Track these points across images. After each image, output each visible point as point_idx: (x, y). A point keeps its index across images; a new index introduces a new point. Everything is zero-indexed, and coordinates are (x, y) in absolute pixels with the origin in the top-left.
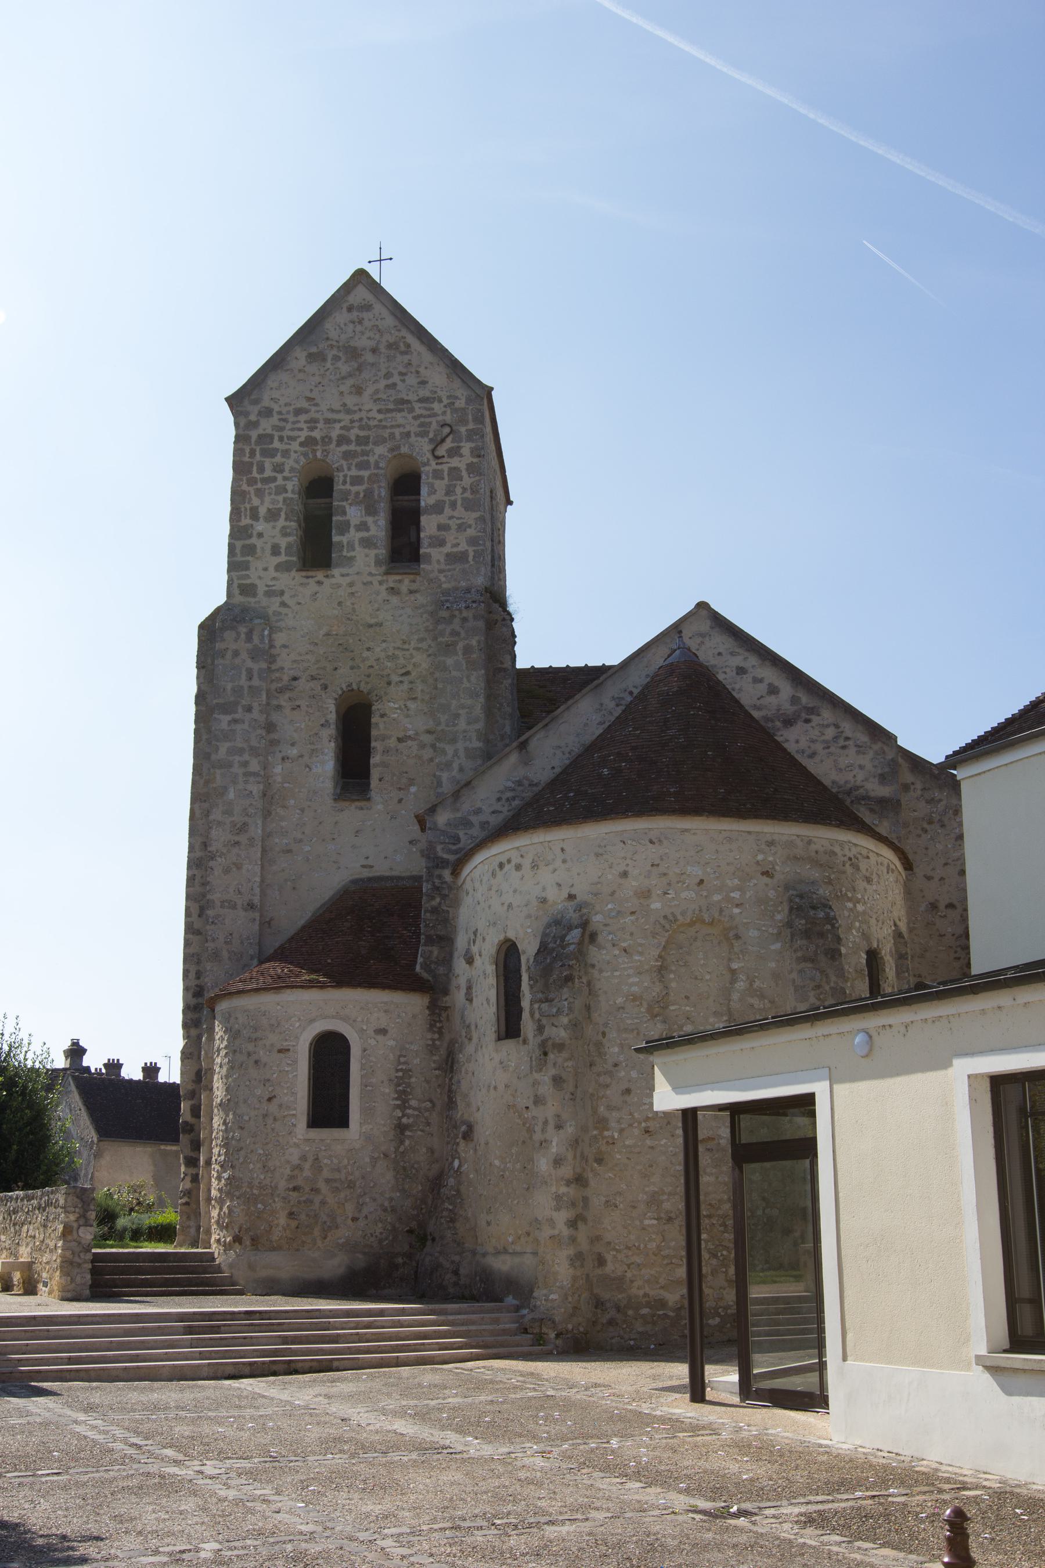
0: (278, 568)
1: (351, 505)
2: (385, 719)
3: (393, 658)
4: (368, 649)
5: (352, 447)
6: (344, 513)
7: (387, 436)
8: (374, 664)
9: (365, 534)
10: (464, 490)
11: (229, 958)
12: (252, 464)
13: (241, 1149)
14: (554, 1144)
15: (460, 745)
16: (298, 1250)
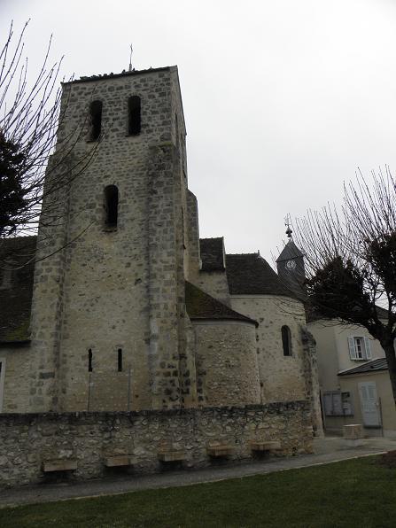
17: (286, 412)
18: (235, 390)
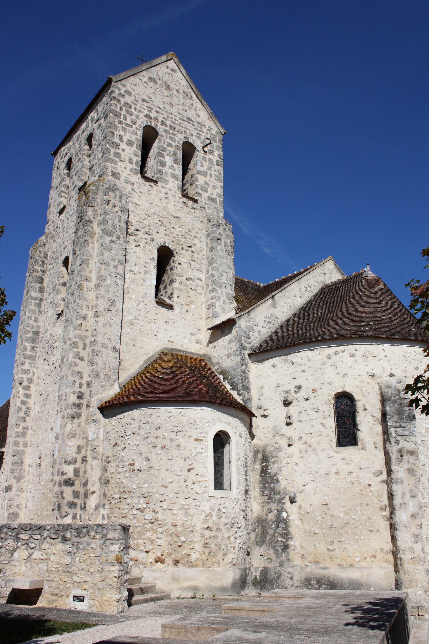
0: (131, 170)
1: (167, 155)
2: (180, 266)
3: (185, 237)
4: (173, 228)
5: (168, 128)
6: (164, 157)
7: (183, 131)
8: (176, 237)
9: (173, 172)
10: (215, 171)
11: (104, 379)
12: (121, 114)
13: (165, 500)
14: (411, 504)
15: (224, 290)
16: (210, 567)
17: (75, 540)
18: (140, 506)
